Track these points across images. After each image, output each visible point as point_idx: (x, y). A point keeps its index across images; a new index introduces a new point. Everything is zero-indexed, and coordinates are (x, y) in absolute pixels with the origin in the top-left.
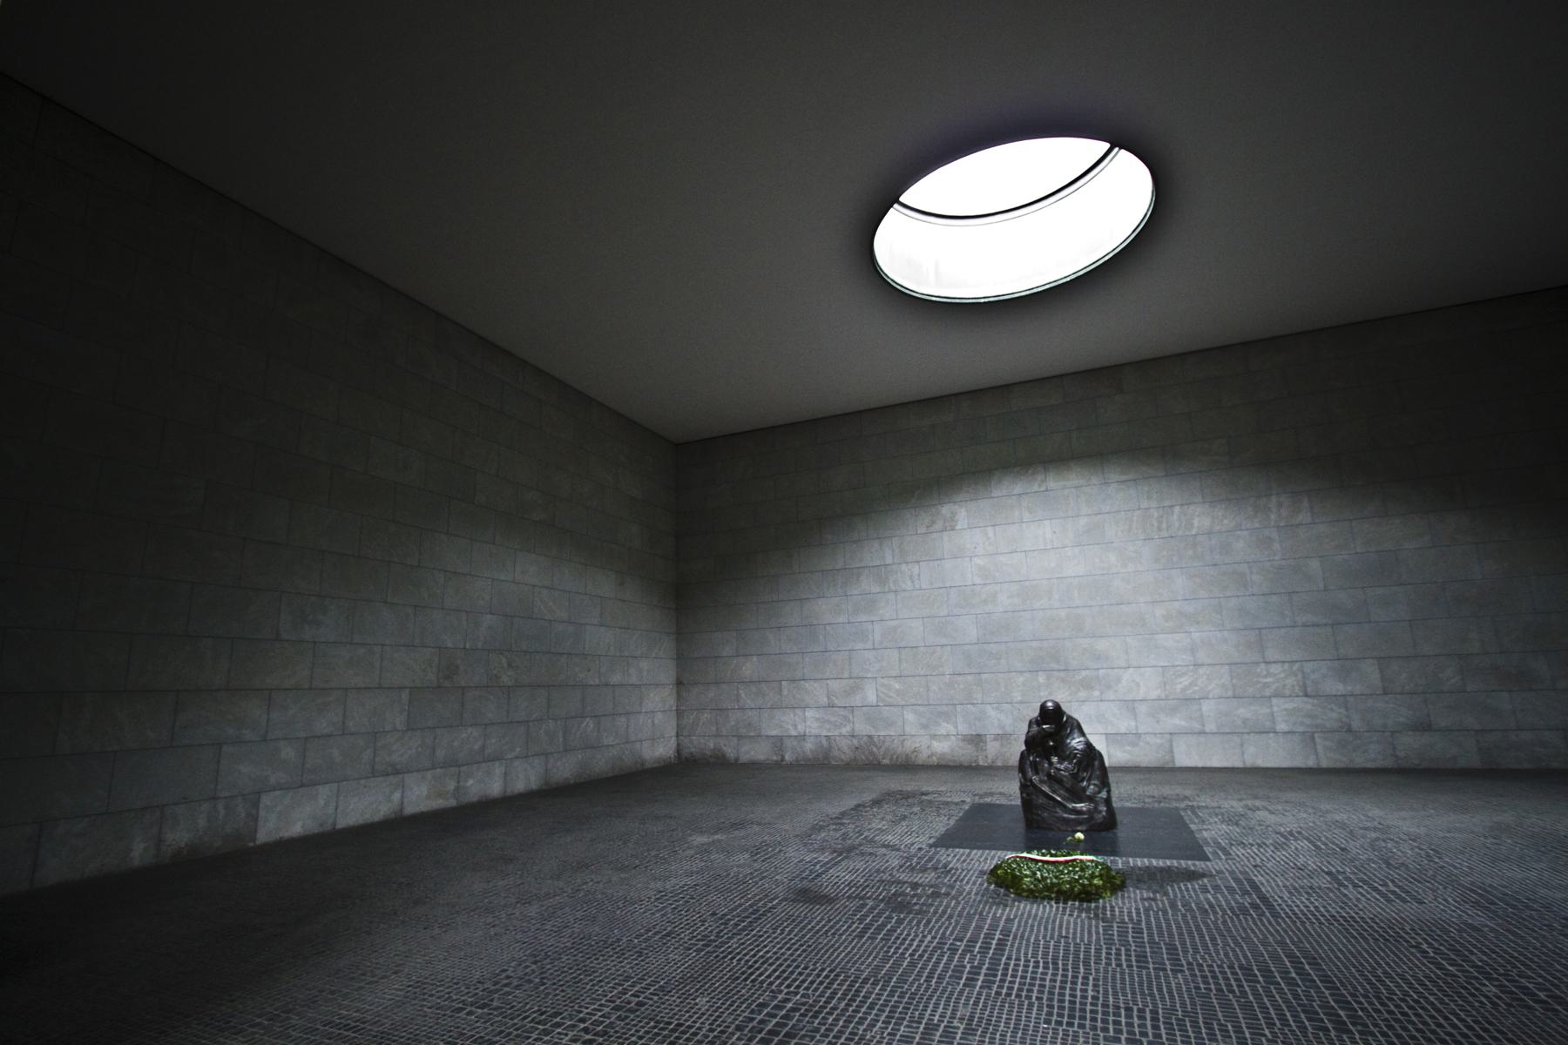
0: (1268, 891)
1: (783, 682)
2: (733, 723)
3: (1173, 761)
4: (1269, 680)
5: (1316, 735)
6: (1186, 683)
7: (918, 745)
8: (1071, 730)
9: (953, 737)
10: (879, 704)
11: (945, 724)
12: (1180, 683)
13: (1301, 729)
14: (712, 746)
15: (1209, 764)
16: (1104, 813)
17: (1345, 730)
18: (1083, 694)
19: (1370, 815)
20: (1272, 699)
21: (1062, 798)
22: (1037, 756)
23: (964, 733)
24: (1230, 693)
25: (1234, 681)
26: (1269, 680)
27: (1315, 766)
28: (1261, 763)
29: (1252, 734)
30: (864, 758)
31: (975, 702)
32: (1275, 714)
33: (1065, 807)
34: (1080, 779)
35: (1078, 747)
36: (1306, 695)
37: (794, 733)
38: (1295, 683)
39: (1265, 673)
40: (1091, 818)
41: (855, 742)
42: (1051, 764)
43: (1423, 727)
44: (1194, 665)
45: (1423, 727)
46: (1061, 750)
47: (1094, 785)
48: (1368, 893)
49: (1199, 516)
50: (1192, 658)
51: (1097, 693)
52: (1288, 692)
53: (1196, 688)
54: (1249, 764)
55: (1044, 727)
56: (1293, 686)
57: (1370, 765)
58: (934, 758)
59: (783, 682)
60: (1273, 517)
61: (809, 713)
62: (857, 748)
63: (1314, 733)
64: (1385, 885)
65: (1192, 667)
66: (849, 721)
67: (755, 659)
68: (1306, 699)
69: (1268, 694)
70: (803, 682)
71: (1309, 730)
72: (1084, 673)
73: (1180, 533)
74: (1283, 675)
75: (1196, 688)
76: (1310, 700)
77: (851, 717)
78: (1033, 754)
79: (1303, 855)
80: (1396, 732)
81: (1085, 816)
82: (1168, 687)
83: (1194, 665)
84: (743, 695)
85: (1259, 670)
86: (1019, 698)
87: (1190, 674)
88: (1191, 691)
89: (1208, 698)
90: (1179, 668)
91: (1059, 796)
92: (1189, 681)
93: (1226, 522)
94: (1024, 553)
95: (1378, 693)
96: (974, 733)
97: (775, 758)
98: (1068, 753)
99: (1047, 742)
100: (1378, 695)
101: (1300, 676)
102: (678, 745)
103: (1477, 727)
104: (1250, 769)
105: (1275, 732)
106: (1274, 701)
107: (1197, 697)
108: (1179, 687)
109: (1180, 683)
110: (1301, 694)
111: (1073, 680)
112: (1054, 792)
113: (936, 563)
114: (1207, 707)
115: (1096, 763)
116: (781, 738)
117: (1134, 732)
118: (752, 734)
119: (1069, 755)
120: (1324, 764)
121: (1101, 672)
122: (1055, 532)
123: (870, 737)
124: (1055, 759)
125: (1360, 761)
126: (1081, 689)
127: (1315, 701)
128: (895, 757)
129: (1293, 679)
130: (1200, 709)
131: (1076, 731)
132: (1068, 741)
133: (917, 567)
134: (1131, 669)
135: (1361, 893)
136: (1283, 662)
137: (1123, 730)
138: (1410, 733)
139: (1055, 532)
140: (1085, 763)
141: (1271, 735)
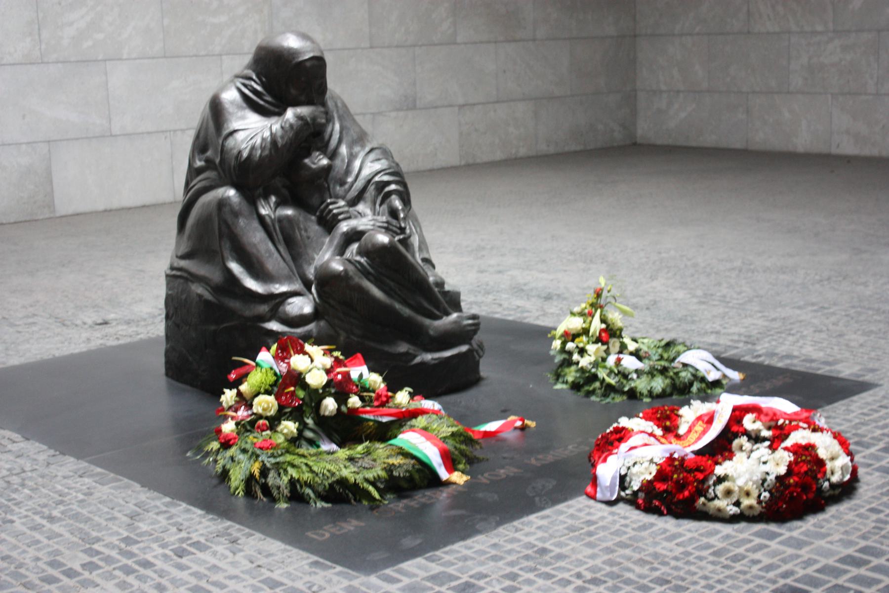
3: (51, 205)
4: (223, 19)
12: (71, 24)
15: (115, 204)
20: (224, 57)
25: (166, 21)
35: (378, 166)
53: (100, 36)
55: (304, 111)
69: (217, 49)
75: (100, 36)
78: (266, 198)
81: (464, 348)
88: (90, 43)
89: (120, 59)
95: (363, 45)
100: (363, 49)
103: (461, 101)
107: (100, 57)
130: (107, 83)
132: (344, 150)
138: (393, 114)
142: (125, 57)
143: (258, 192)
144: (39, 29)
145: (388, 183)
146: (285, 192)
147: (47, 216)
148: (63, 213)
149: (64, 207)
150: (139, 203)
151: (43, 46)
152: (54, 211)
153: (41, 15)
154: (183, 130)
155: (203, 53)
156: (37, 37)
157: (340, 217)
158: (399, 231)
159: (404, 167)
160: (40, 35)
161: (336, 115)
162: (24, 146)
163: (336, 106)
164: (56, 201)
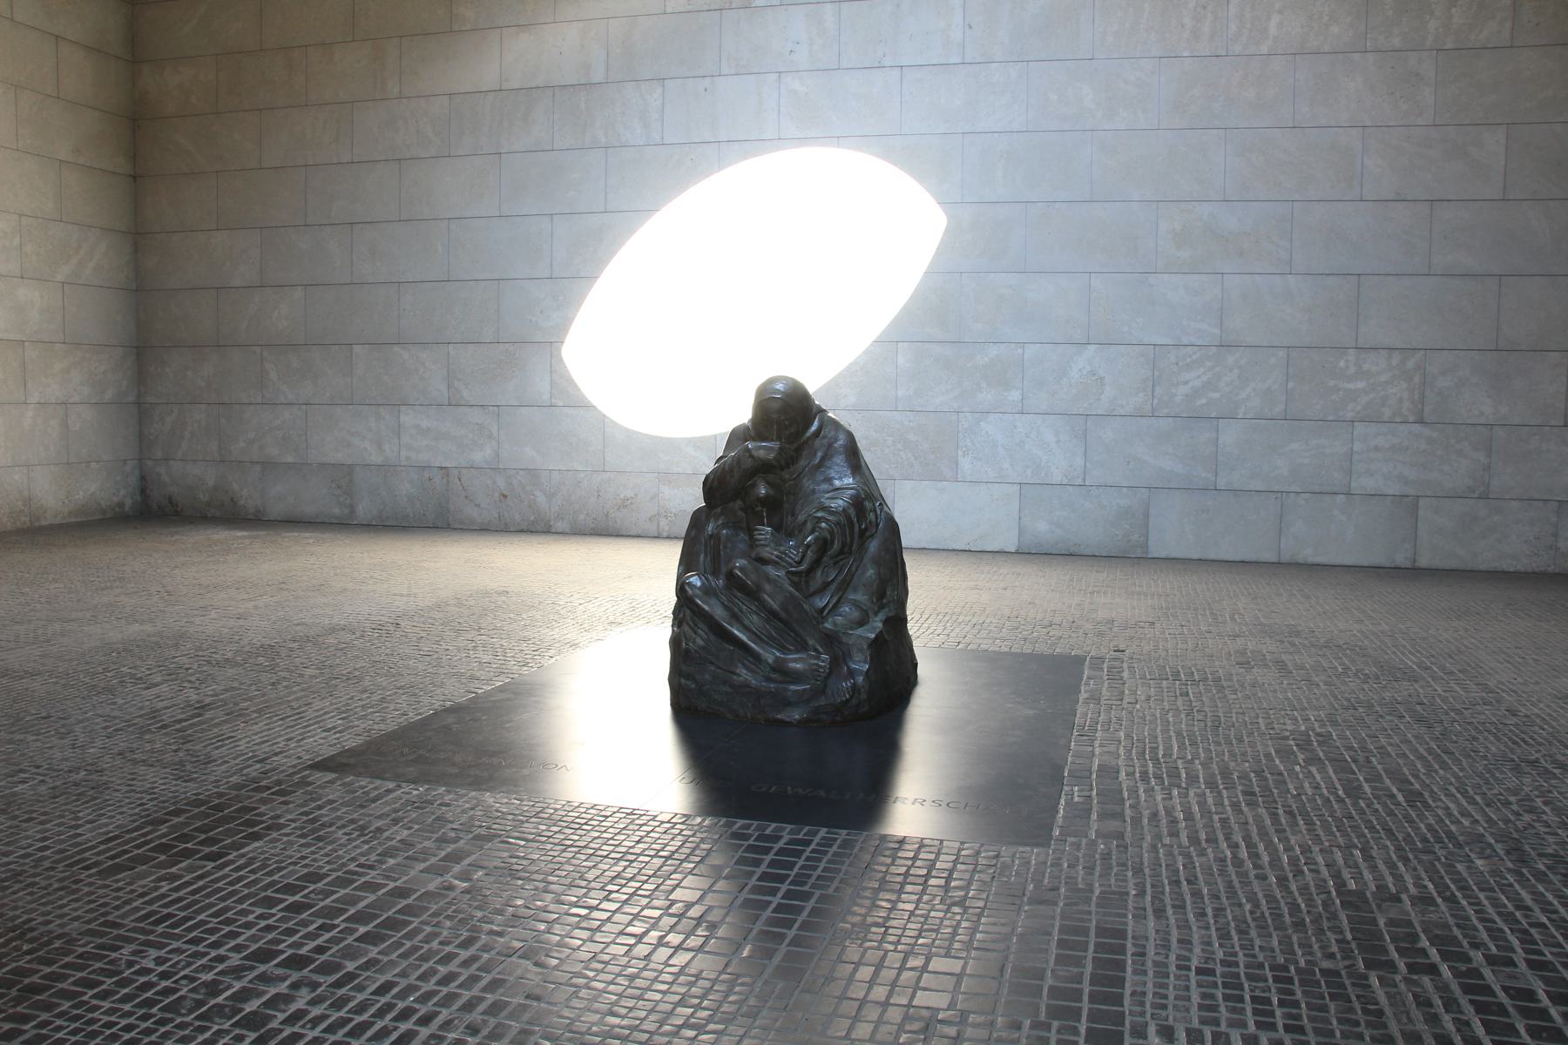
0: (1139, 996)
1: (357, 349)
2: (251, 435)
3: (1145, 546)
4: (1360, 385)
5: (1421, 502)
6: (1198, 383)
7: (630, 494)
8: (823, 459)
10: (553, 400)
12: (1186, 383)
13: (1394, 488)
14: (211, 483)
15: (1212, 556)
16: (860, 679)
18: (986, 397)
19: (1491, 684)
21: (756, 637)
22: (724, 526)
24: (1279, 408)
25: (1291, 385)
26: (1360, 385)
28: (1308, 555)
30: (517, 517)
32: (1355, 457)
33: (757, 658)
34: (814, 586)
36: (1421, 422)
37: (376, 458)
38: (1406, 395)
39: (1352, 370)
40: (821, 691)
41: (501, 482)
42: (753, 543)
46: (779, 510)
47: (856, 604)
48: (1450, 1004)
49: (1280, 12)
50: (1217, 331)
51: (1015, 395)
52: (1387, 413)
53: (1216, 395)
54: (1286, 558)
56: (1401, 400)
57: (1507, 565)
58: (663, 523)
59: (357, 349)
60: (1433, 25)
61: (408, 418)
62: (505, 496)
64: (1502, 961)
65: (1214, 349)
66: (490, 436)
67: (298, 293)
68: (1417, 428)
69: (1350, 415)
70: (396, 348)
71: (1412, 491)
72: (994, 351)
73: (1237, 49)
74: (1383, 378)
75: (1216, 395)
76: (1427, 431)
77: (494, 430)
79: (1309, 823)
82: (1158, 390)
84: (273, 375)
85: (1342, 364)
87: (1208, 364)
88: (1204, 401)
91: (746, 629)
92: (1205, 378)
93: (1335, 29)
94: (896, 72)
95: (1553, 423)
97: (337, 511)
98: (801, 518)
99: (754, 486)
101: (1417, 380)
102: (143, 478)
104: (1289, 564)
106: (1360, 428)
108: (1183, 390)
109: (1186, 383)
111: (969, 365)
112: (735, 618)
113: (707, 81)
114: (1230, 436)
115: (873, 546)
116: (348, 470)
117: (1079, 481)
118: (290, 459)
119: (805, 522)
120: (1424, 561)
121: (1030, 351)
122: (970, 27)
123: (533, 473)
124: (765, 531)
125: (1486, 557)
126: (984, 385)
127: (1435, 435)
128: (582, 517)
129: (1404, 385)
131: (839, 460)
133: (659, 91)
134: (1092, 348)
135: (1424, 1003)
137: (1057, 477)
139: (970, 27)
140: (836, 546)
145: (820, 520)
147: (1139, 556)
148: (1155, 555)
149: (1156, 550)
150: (1237, 558)
151: (1156, 401)
152: (1147, 553)
153: (1157, 373)
154: (1298, 493)
155: (1331, 418)
156: (1150, 393)
157: (757, 543)
158: (795, 564)
160: (1153, 391)
161: (819, 454)
162: (1125, 490)
163: (830, 445)
164: (1150, 543)
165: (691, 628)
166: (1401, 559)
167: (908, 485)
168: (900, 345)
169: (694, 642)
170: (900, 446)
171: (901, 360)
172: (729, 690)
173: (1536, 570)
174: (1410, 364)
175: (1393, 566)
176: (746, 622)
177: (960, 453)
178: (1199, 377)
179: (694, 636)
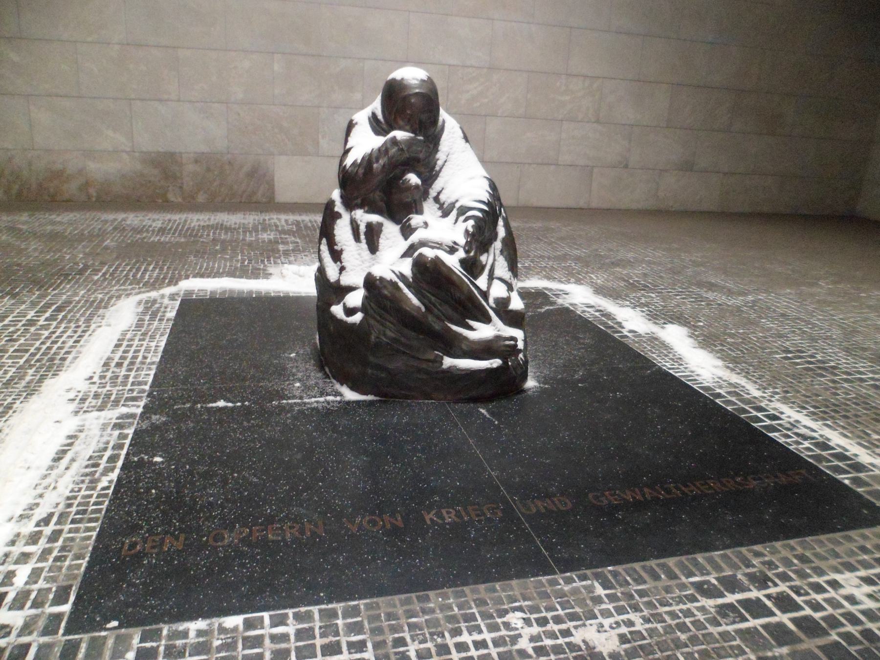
4: (567, 98)
5: (596, 170)
9: (125, 156)
11: (110, 133)
12: (468, 92)
17: (622, 166)
23: (144, 149)
27: (585, 206)
28: (535, 202)
29: (535, 166)
31: (166, 97)
36: (598, 121)
43: (687, 167)
44: (489, 68)
45: (687, 167)
53: (486, 100)
57: (634, 206)
58: (92, 191)
63: (593, 167)
65: (485, 70)
68: (595, 125)
80: (666, 171)
83: (489, 68)
85: (558, 84)
86: (241, 96)
88: (478, 104)
90: (470, 70)
96: (161, 150)
105: (557, 165)
110: (593, 120)
120: (594, 205)
128: (16, 187)
130: (485, 129)
136: (586, 77)
141: (552, 168)
142: (499, 115)
143: (356, 202)
144: (448, 93)
146: (382, 204)
154: (530, 164)
159: (507, 199)
160: (448, 97)
165: (378, 321)
166: (582, 203)
167: (283, 159)
168: (276, 55)
169: (385, 335)
170: (276, 130)
171: (276, 67)
172: (425, 377)
173: (649, 208)
174: (595, 85)
175: (578, 207)
176: (436, 311)
177: (320, 137)
178: (475, 88)
179: (383, 329)
